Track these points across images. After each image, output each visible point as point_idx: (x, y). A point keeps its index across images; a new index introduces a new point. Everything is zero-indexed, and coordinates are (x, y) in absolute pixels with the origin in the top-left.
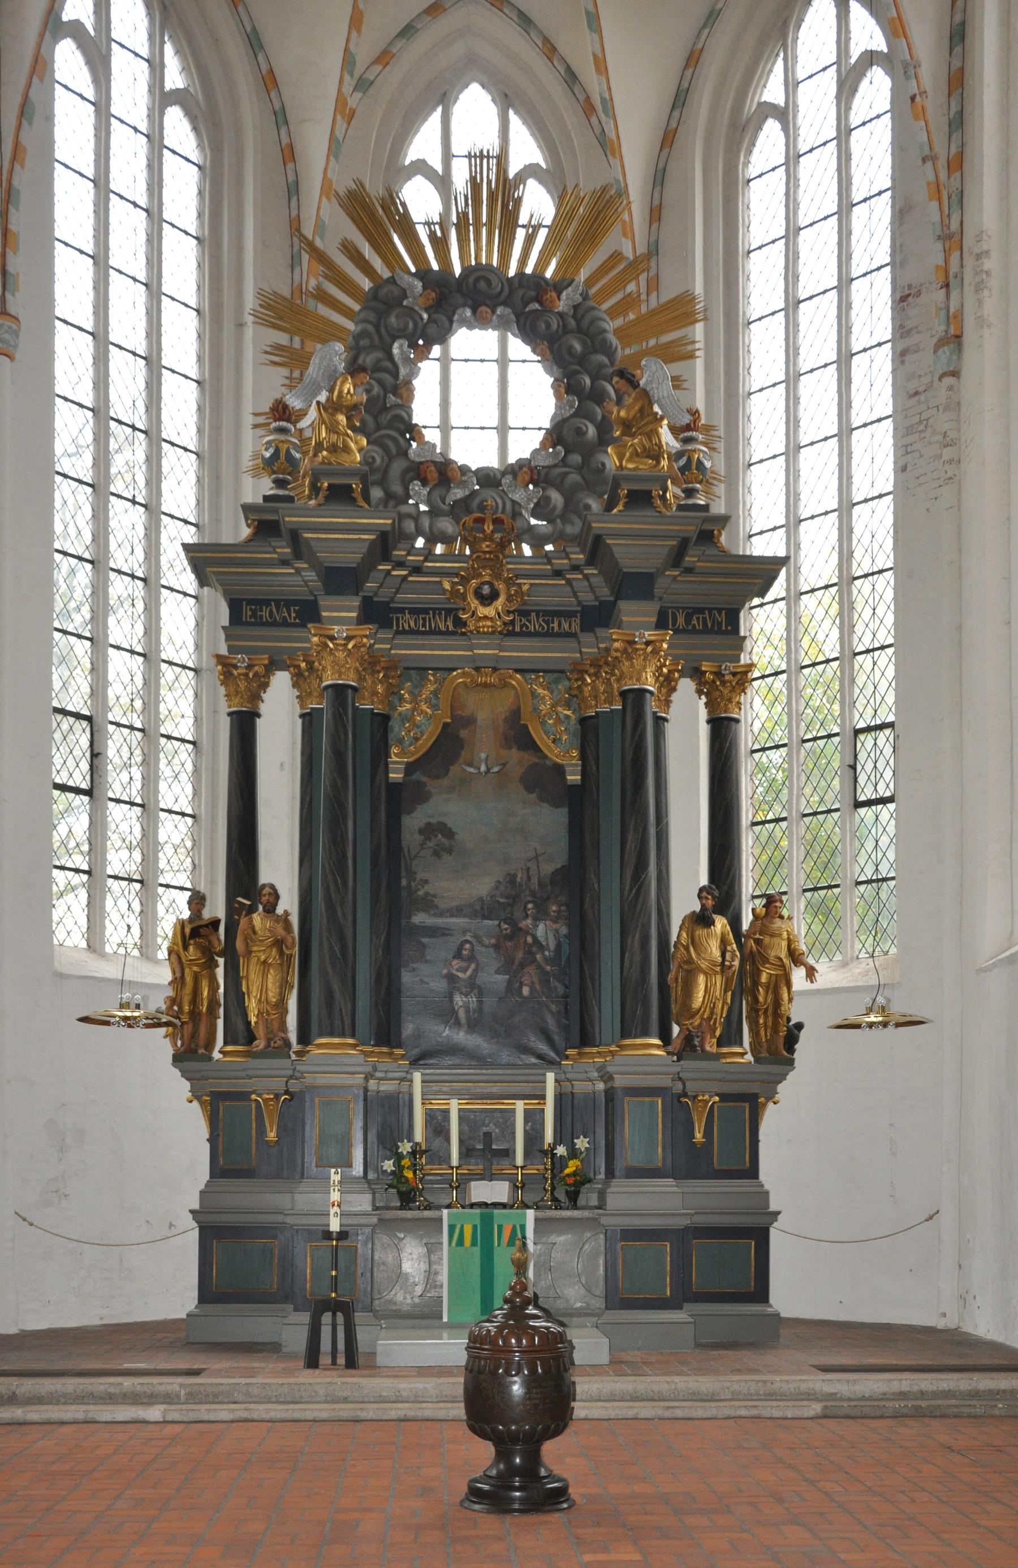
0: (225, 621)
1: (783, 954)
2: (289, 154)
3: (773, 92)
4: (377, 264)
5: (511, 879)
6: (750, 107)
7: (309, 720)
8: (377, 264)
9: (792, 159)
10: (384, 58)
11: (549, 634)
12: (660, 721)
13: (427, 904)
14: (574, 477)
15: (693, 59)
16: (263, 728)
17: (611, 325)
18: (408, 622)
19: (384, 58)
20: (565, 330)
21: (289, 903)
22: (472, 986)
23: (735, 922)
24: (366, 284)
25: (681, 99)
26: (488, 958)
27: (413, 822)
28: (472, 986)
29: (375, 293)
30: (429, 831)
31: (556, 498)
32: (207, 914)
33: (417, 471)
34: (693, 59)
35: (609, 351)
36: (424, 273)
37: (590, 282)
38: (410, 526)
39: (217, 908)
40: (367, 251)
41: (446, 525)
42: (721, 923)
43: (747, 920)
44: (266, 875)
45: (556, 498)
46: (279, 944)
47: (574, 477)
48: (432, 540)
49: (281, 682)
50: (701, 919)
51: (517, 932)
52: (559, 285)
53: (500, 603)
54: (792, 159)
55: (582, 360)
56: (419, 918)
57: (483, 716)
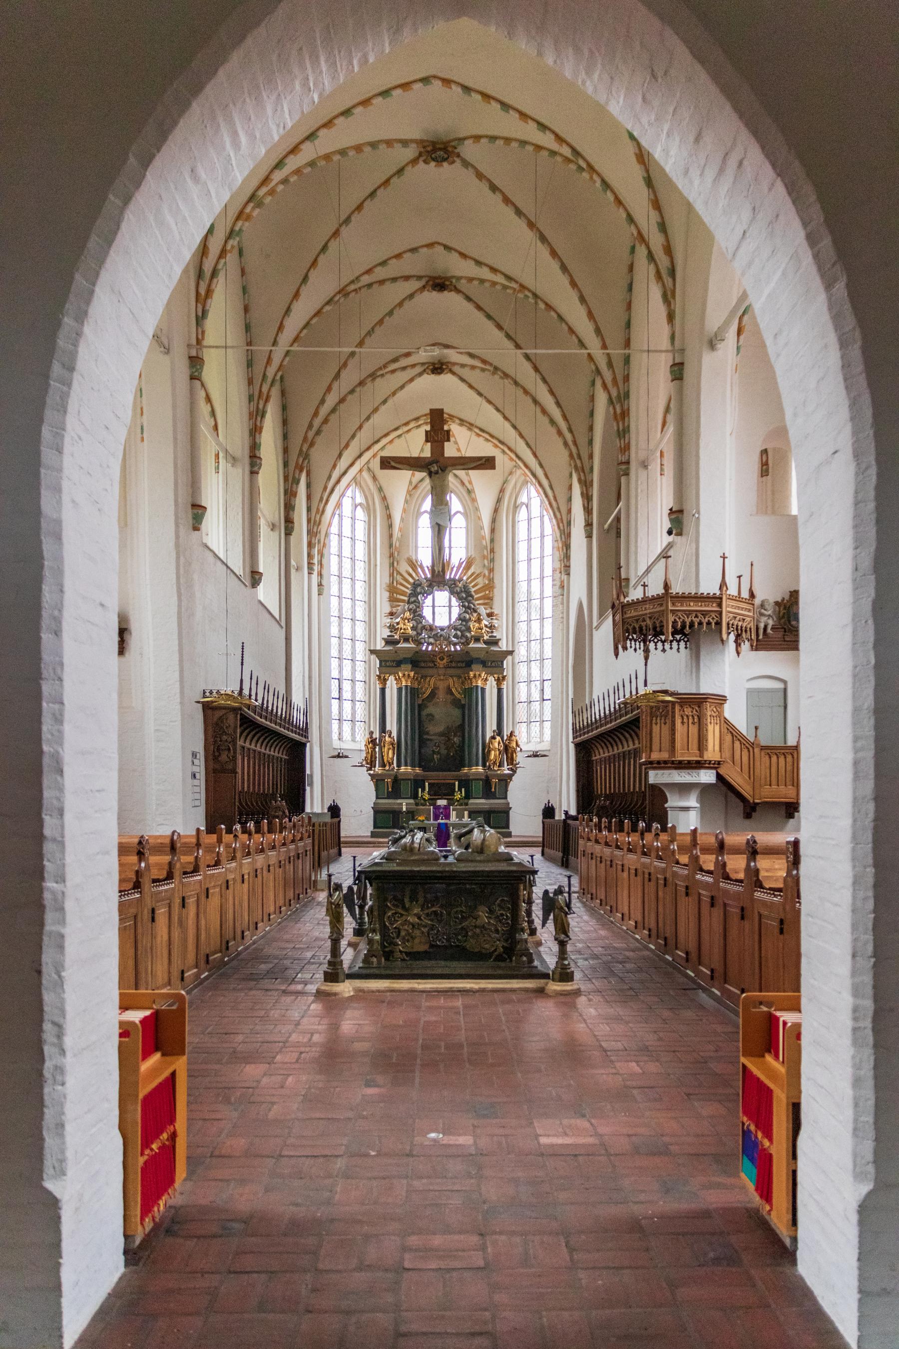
0: (378, 666)
1: (514, 745)
2: (389, 517)
3: (523, 498)
4: (414, 575)
5: (448, 727)
6: (519, 502)
7: (400, 690)
8: (414, 575)
9: (529, 520)
10: (416, 487)
11: (458, 667)
12: (483, 690)
13: (428, 733)
14: (464, 628)
15: (502, 491)
16: (388, 691)
17: (473, 590)
18: (423, 664)
19: (416, 487)
20: (461, 591)
21: (394, 734)
22: (438, 753)
23: (502, 738)
24: (411, 580)
25: (499, 500)
26: (442, 746)
27: (424, 713)
28: (438, 753)
29: (414, 583)
30: (428, 715)
31: (459, 633)
32: (374, 736)
33: (424, 627)
34: (502, 491)
35: (472, 596)
36: (426, 578)
37: (468, 579)
38: (423, 641)
39: (376, 735)
40: (411, 571)
41: (431, 640)
42: (498, 738)
43: (505, 738)
44: (388, 728)
45: (459, 633)
46: (392, 744)
47: (464, 628)
48: (429, 644)
49: (392, 678)
50: (493, 738)
51: (449, 739)
52: (460, 580)
53: (445, 661)
54: (529, 520)
55: (466, 599)
56: (425, 737)
57: (441, 687)
